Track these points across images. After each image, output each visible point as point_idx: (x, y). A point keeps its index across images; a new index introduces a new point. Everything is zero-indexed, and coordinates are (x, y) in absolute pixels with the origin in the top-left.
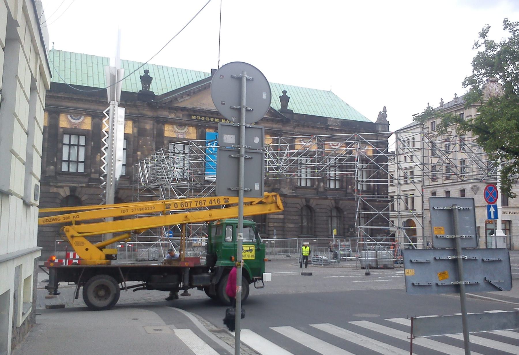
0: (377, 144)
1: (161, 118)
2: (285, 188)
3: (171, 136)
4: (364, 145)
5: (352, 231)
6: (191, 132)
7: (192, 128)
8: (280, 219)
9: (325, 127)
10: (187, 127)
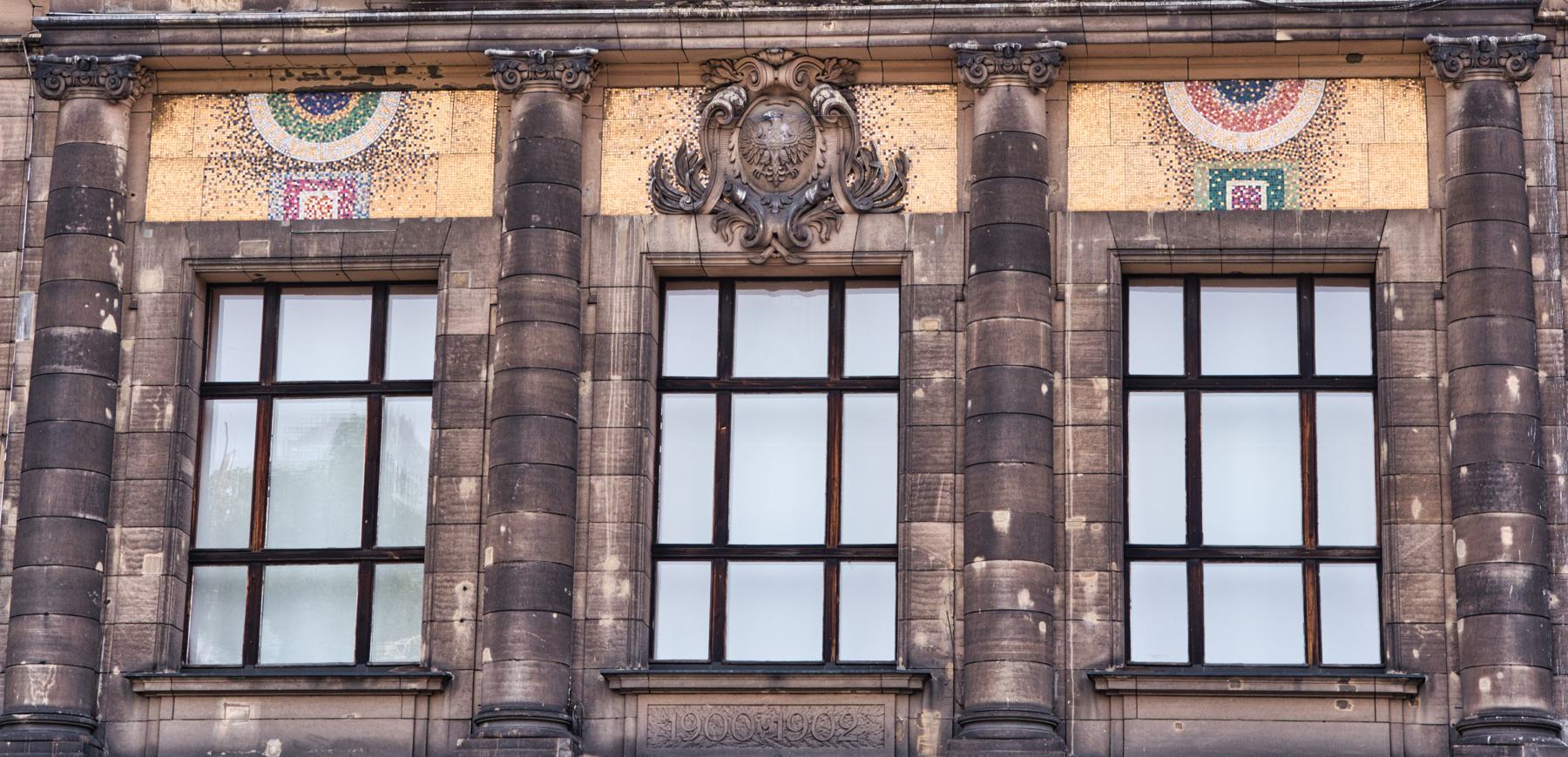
1: (75, 37)
3: (213, 216)
6: (435, 146)
7: (443, 100)
10: (390, 100)
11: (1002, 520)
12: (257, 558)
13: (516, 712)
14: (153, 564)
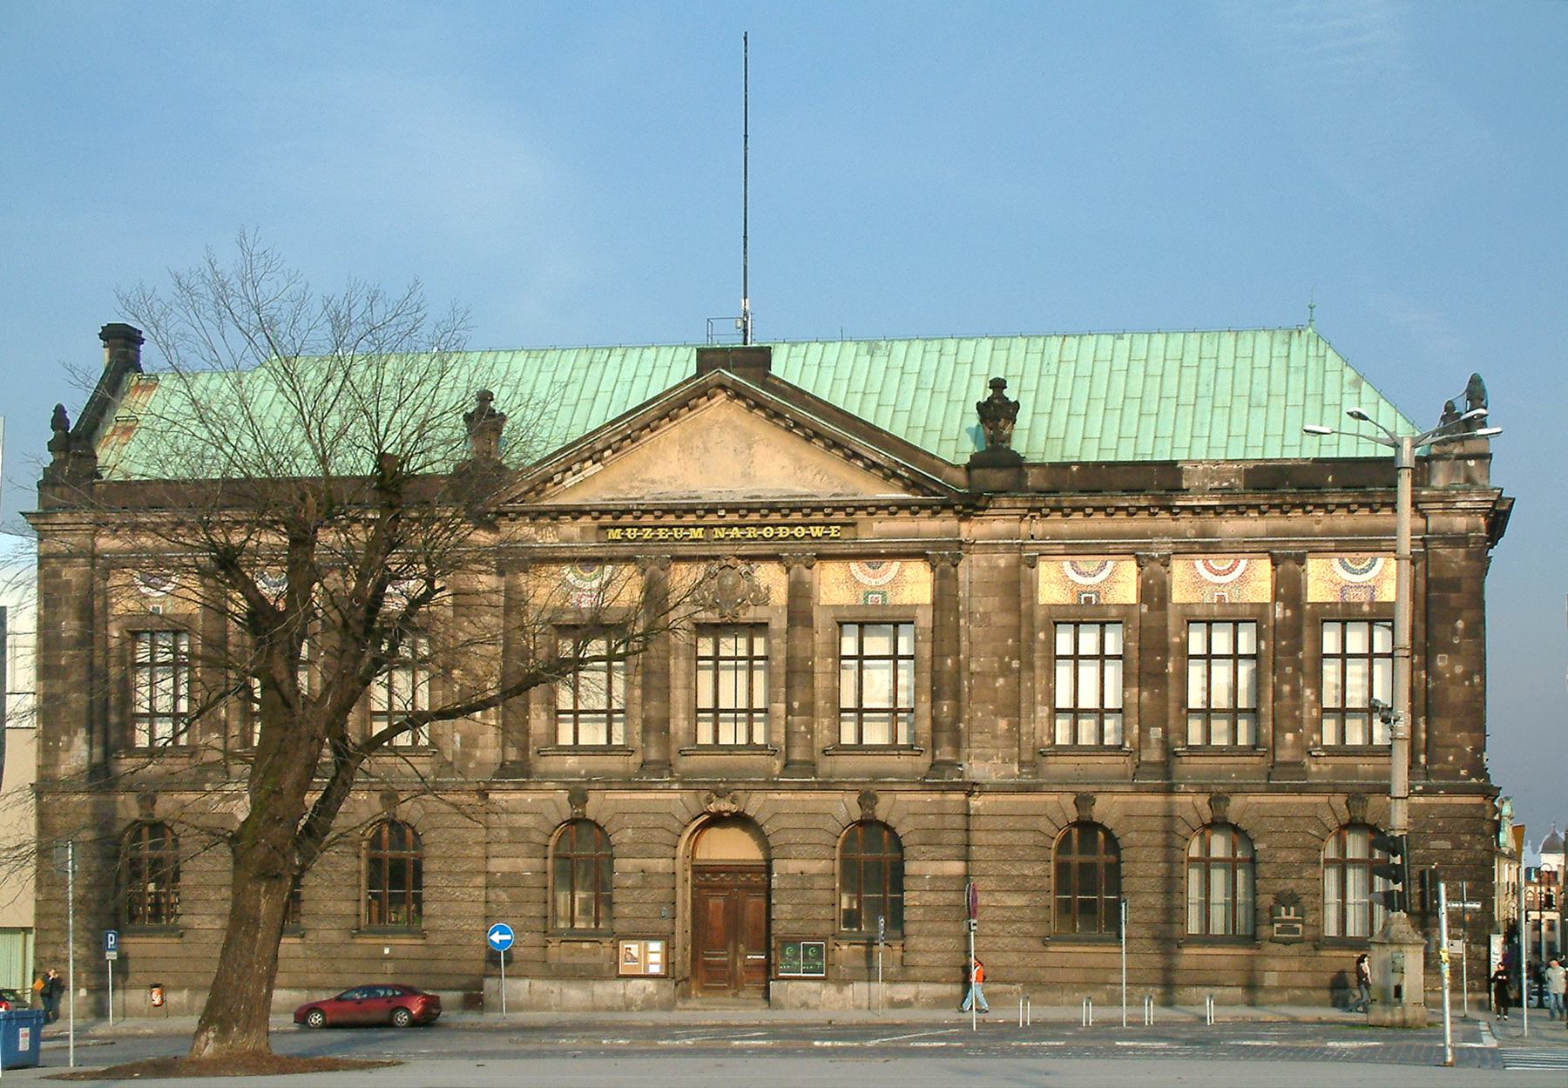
0: (1425, 546)
2: (987, 759)
4: (1361, 554)
5: (1292, 917)
8: (950, 878)
9: (1152, 503)
11: (796, 705)
12: (576, 712)
13: (651, 762)
14: (544, 716)
